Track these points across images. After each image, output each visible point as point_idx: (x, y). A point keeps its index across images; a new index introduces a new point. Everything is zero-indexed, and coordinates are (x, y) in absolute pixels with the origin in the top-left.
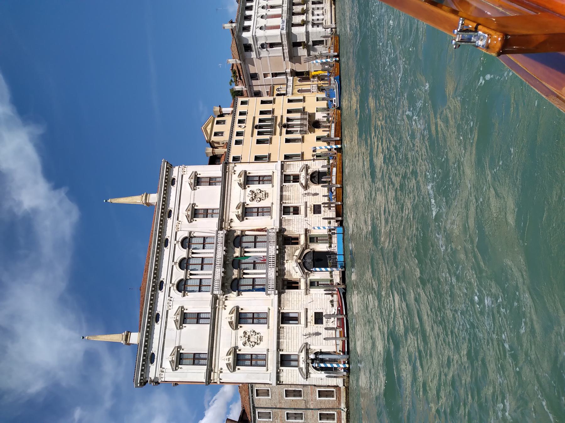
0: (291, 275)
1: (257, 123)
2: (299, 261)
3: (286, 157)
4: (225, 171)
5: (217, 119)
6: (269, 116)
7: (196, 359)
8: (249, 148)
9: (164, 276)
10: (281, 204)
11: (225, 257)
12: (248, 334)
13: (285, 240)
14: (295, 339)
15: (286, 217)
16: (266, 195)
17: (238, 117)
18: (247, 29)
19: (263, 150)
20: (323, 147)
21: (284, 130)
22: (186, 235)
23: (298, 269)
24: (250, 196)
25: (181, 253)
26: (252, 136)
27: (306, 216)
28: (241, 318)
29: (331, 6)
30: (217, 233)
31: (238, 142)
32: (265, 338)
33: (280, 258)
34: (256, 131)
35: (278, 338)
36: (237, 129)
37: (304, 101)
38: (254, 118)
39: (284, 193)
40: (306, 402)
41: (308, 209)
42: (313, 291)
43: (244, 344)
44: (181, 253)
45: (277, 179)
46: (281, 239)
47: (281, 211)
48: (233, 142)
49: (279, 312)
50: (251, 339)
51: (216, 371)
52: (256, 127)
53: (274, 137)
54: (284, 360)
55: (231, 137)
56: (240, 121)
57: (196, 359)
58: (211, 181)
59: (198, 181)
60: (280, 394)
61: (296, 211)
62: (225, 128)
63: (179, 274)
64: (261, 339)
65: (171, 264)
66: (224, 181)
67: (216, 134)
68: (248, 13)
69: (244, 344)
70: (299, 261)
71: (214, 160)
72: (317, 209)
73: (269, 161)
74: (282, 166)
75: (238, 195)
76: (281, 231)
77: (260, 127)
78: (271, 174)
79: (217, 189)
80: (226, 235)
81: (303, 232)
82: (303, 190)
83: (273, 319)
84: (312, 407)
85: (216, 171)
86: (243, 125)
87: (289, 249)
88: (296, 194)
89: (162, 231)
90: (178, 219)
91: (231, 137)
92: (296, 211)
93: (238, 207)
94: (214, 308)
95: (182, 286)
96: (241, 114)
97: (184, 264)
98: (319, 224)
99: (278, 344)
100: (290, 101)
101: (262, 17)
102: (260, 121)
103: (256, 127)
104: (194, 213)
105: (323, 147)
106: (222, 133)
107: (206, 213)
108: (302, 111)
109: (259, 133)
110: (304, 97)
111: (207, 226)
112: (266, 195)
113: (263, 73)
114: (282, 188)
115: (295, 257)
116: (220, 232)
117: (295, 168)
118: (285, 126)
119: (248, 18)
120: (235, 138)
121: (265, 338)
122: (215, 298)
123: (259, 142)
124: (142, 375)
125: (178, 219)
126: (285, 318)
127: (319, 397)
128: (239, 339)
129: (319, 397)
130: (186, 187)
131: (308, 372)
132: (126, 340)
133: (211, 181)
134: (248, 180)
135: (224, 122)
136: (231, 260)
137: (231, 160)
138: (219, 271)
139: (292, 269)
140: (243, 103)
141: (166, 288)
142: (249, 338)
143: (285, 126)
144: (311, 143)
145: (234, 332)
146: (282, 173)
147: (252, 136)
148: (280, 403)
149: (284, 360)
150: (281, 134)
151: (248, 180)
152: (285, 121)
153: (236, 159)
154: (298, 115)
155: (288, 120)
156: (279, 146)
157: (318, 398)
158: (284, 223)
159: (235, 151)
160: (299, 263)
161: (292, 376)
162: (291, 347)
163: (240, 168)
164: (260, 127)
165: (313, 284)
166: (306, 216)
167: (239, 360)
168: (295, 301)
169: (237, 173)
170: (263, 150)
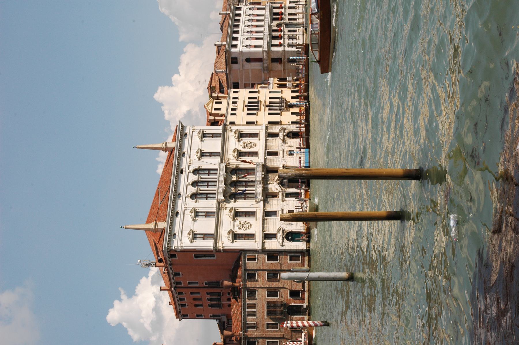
0: (272, 190)
1: (246, 104)
2: (278, 182)
3: (269, 123)
4: (225, 130)
5: (215, 101)
6: (256, 100)
7: (206, 236)
8: (241, 117)
9: (181, 190)
10: (266, 150)
11: (226, 180)
12: (242, 223)
13: (268, 170)
14: (274, 225)
15: (270, 157)
16: (255, 145)
17: (232, 100)
18: (235, 46)
19: (251, 119)
20: (295, 118)
21: (267, 108)
22: (197, 167)
23: (278, 187)
24: (243, 145)
25: (193, 178)
26: (243, 111)
27: (283, 157)
28: (237, 214)
29: (303, 35)
30: (220, 166)
31: (232, 114)
32: (255, 226)
33: (265, 181)
34: (246, 108)
35: (263, 224)
36: (231, 106)
37: (282, 93)
38: (244, 101)
39: (268, 144)
40: (281, 265)
41: (285, 153)
42: (287, 199)
43: (240, 228)
44: (193, 178)
45: (262, 135)
46: (265, 170)
47: (265, 153)
48: (229, 114)
49: (264, 210)
50: (244, 226)
51: (220, 242)
52: (246, 106)
53: (259, 112)
54: (268, 236)
55: (227, 111)
56: (233, 103)
57: (206, 236)
58: (214, 135)
59: (204, 135)
60: (264, 259)
61: (276, 154)
62: (223, 106)
63: (192, 190)
64: (251, 226)
65: (186, 183)
66: (223, 136)
67: (216, 109)
68: (235, 35)
69: (240, 228)
70: (278, 182)
71: (214, 123)
72: (291, 154)
73: (257, 125)
74: (267, 127)
75: (233, 143)
76: (264, 166)
77: (249, 106)
78: (258, 132)
79: (219, 140)
80: (226, 168)
81: (281, 166)
82: (282, 141)
83: (260, 214)
84: (285, 269)
85: (219, 129)
86: (236, 105)
87: (271, 175)
88: (276, 144)
89: (179, 164)
90: (190, 158)
91: (227, 111)
92: (276, 154)
93: (234, 151)
94: (219, 209)
95: (194, 196)
96: (234, 98)
97: (195, 184)
98: (293, 162)
99: (263, 228)
100: (270, 92)
101: (247, 39)
102: (249, 103)
103: (246, 106)
104: (202, 154)
105: (295, 118)
106: (220, 109)
107: (211, 154)
108: (281, 98)
109: (248, 109)
110: (282, 91)
111: (213, 162)
112: (255, 145)
113: (244, 83)
114: (266, 140)
115: (275, 180)
116: (222, 164)
117: (275, 129)
118: (268, 106)
119: (236, 39)
120: (230, 112)
121: (255, 226)
122: (219, 203)
123: (248, 114)
124: (168, 244)
125: (190, 158)
126: (267, 214)
127: (290, 261)
128: (236, 226)
129: (290, 261)
130: (196, 138)
131: (283, 242)
132: (155, 226)
133: (214, 135)
134: (241, 135)
135: (221, 103)
136: (229, 182)
137: (228, 123)
138: (222, 187)
139: (274, 187)
140: (235, 92)
141: (182, 198)
142: (243, 226)
143: (268, 106)
144: (287, 118)
145: (232, 222)
146: (266, 132)
147: (243, 111)
148: (263, 265)
149: (268, 236)
150: (265, 111)
151: (241, 135)
152: (267, 103)
153: (232, 123)
154: (278, 100)
155: (270, 103)
156: (263, 117)
157: (289, 262)
158: (267, 161)
159: (231, 118)
160: (278, 183)
161: (273, 245)
162: (271, 229)
163: (234, 128)
164: (249, 106)
165: (288, 195)
166: (283, 157)
167: (236, 237)
168: (274, 205)
169: (234, 131)
170: (251, 119)
